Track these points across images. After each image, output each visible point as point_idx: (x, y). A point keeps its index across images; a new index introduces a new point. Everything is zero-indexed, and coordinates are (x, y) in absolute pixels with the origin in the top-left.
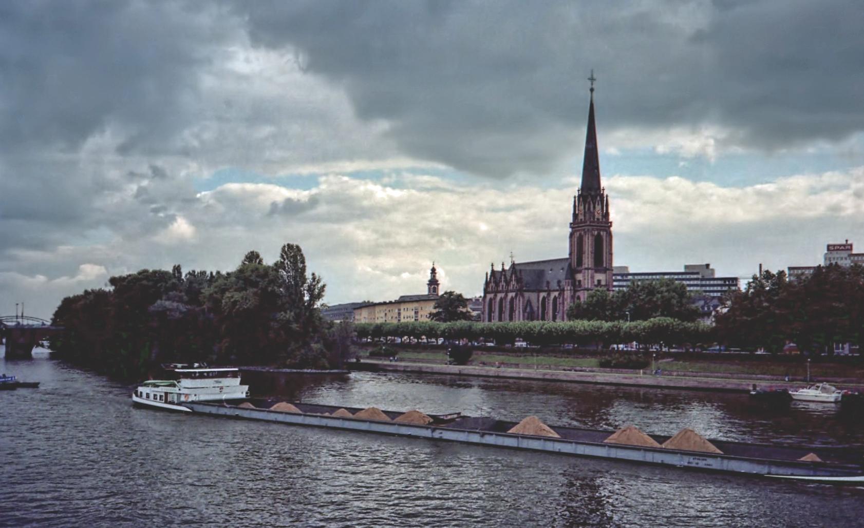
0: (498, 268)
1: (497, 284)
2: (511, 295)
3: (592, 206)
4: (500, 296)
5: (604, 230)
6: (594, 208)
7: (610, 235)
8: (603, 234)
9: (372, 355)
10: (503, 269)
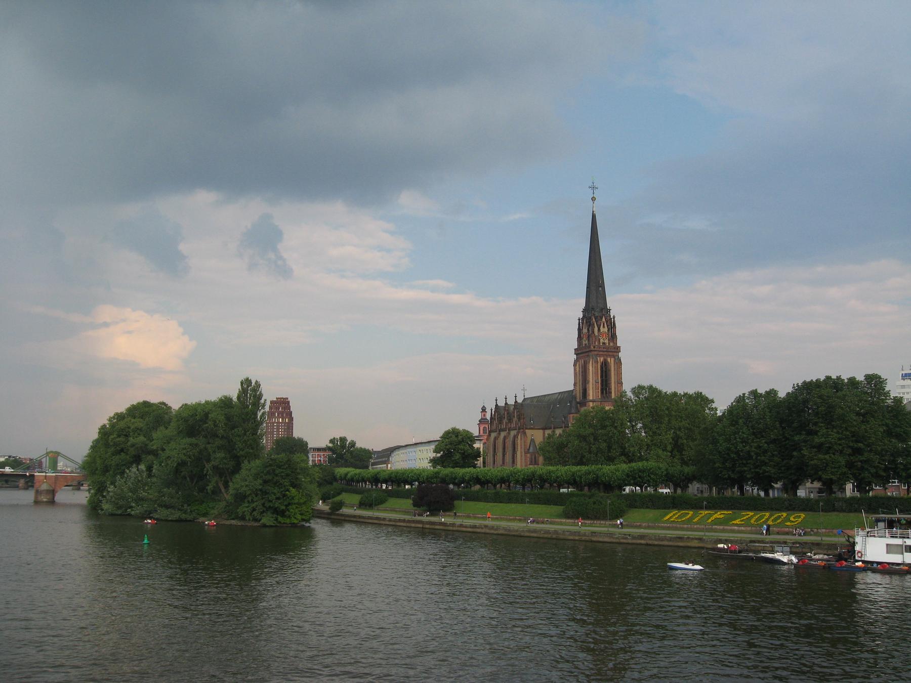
0: (501, 403)
1: (500, 422)
2: (513, 433)
3: (596, 329)
4: (503, 434)
5: (611, 356)
6: (599, 330)
7: (619, 362)
8: (611, 361)
9: (362, 505)
10: (506, 404)
